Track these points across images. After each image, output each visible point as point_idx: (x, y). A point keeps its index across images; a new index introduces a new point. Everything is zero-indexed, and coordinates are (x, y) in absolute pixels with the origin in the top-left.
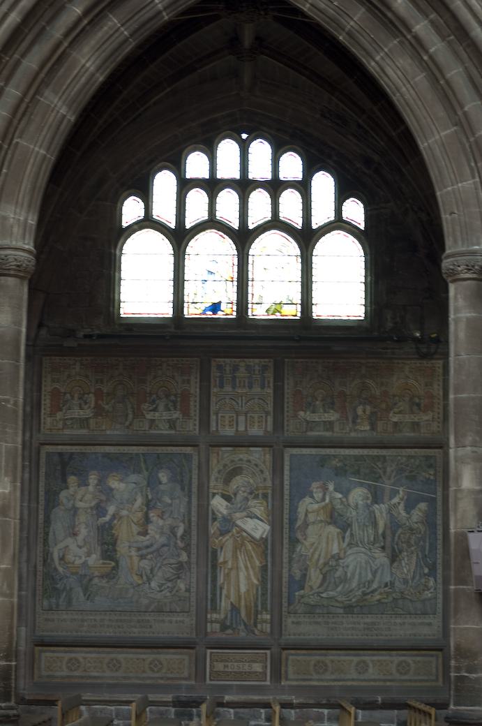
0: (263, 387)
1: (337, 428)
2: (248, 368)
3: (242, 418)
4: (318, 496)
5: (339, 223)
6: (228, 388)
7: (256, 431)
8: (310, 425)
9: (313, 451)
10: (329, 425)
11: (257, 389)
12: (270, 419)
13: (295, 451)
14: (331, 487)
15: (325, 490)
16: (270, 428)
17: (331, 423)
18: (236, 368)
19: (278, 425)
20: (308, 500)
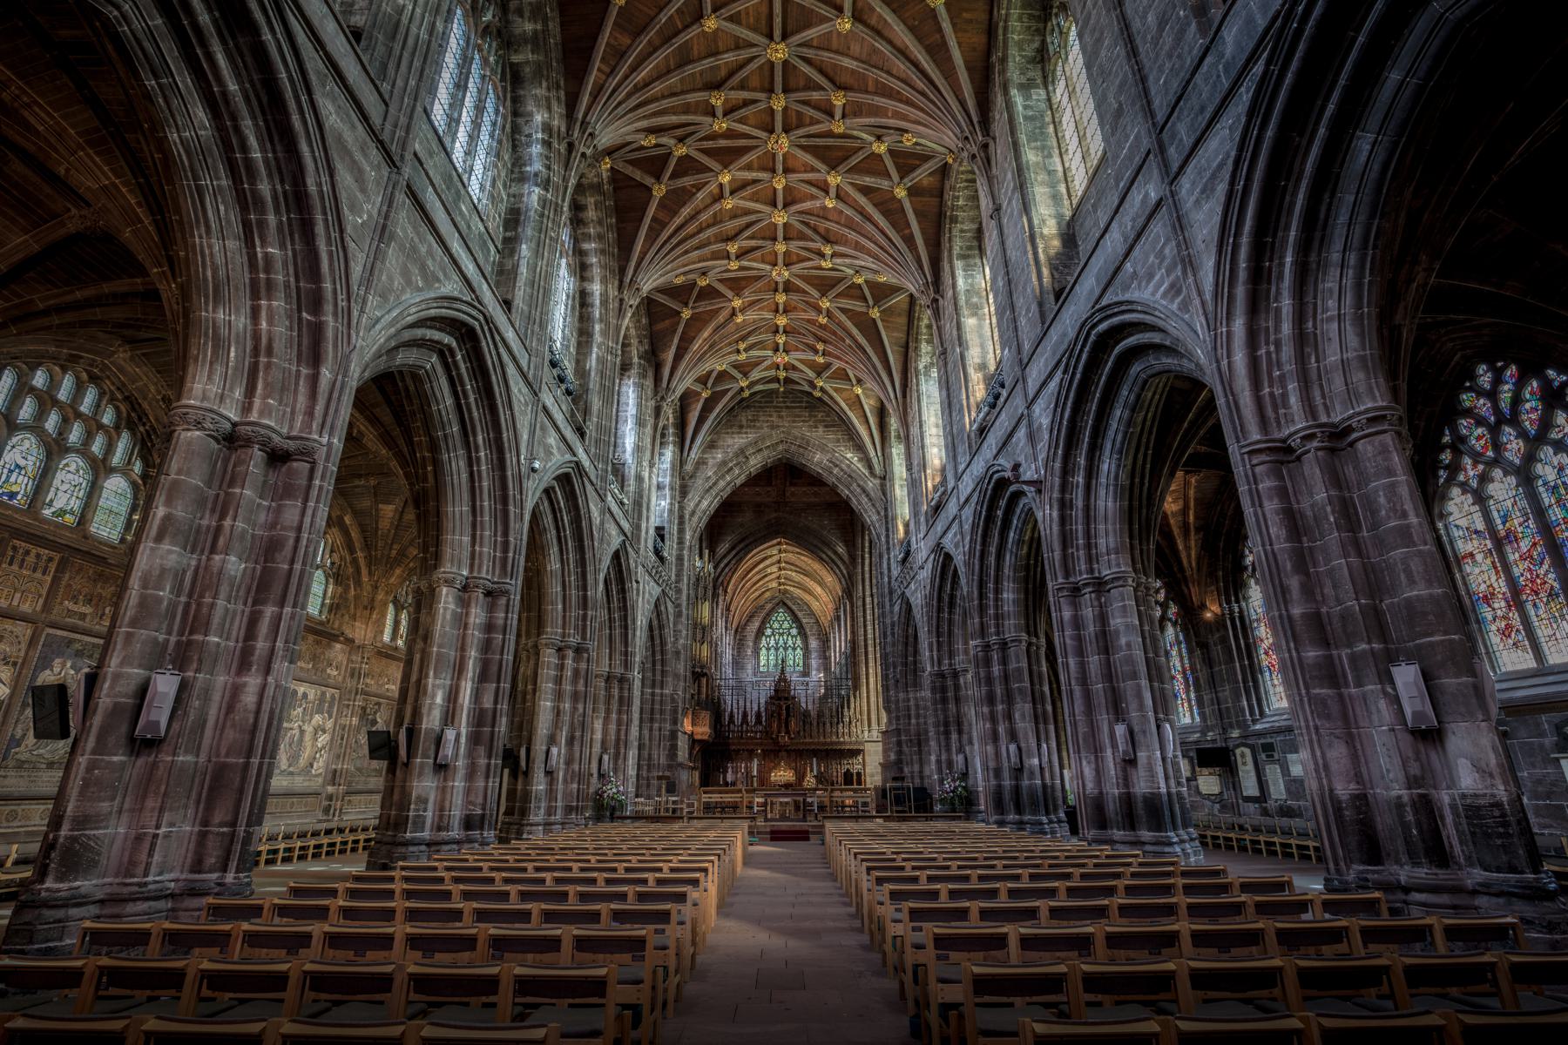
0: (44, 574)
1: (87, 620)
2: (38, 556)
3: (18, 595)
4: (57, 670)
5: (125, 471)
6: (15, 567)
7: (26, 608)
8: (70, 613)
9: (65, 634)
10: (83, 616)
11: (38, 575)
12: (41, 601)
13: (51, 631)
14: (69, 665)
15: (64, 665)
16: (39, 608)
17: (85, 615)
18: (27, 553)
19: (47, 607)
20: (48, 672)
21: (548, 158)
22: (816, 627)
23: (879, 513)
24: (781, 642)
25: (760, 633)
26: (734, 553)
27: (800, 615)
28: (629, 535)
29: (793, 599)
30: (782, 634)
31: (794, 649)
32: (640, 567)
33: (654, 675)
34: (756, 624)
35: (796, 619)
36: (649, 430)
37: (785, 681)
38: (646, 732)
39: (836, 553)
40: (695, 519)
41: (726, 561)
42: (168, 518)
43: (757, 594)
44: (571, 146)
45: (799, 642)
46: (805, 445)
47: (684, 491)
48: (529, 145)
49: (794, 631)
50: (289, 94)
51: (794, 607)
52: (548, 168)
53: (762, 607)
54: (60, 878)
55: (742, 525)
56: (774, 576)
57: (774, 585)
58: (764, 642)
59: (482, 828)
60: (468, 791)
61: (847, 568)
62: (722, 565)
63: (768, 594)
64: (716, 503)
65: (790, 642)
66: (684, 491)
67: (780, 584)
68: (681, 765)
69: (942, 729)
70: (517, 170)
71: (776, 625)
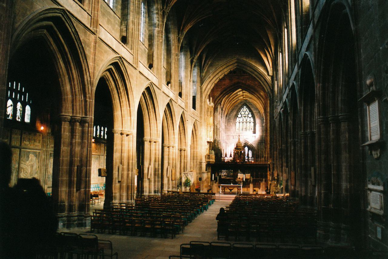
21: (158, 18)
22: (259, 114)
23: (270, 88)
24: (245, 120)
25: (236, 116)
26: (222, 95)
27: (252, 109)
28: (184, 107)
29: (249, 102)
30: (245, 117)
31: (250, 123)
32: (188, 116)
33: (194, 145)
34: (235, 113)
35: (251, 111)
36: (189, 69)
37: (240, 142)
38: (192, 163)
39: (260, 95)
40: (206, 91)
41: (219, 98)
42: (116, 149)
43: (235, 101)
44: (164, 12)
45: (252, 120)
46: (245, 64)
47: (202, 82)
48: (153, 14)
49: (250, 115)
50: (124, 73)
51: (250, 106)
52: (158, 21)
53: (237, 106)
54: (115, 200)
55: (224, 85)
56: (240, 95)
57: (242, 97)
58: (238, 119)
59: (158, 193)
60: (155, 185)
61: (264, 100)
62: (217, 100)
63: (239, 101)
64: (213, 86)
65: (248, 120)
66: (202, 82)
67: (244, 97)
68: (203, 173)
69: (281, 166)
70: (150, 22)
71: (243, 113)
